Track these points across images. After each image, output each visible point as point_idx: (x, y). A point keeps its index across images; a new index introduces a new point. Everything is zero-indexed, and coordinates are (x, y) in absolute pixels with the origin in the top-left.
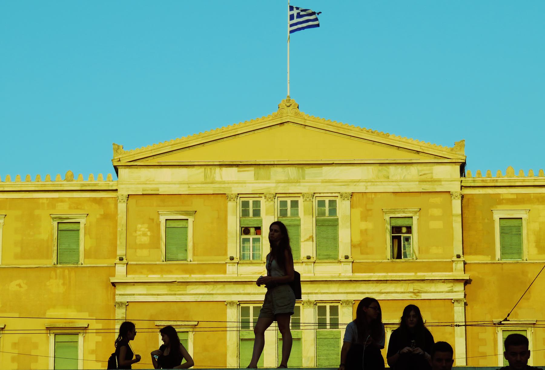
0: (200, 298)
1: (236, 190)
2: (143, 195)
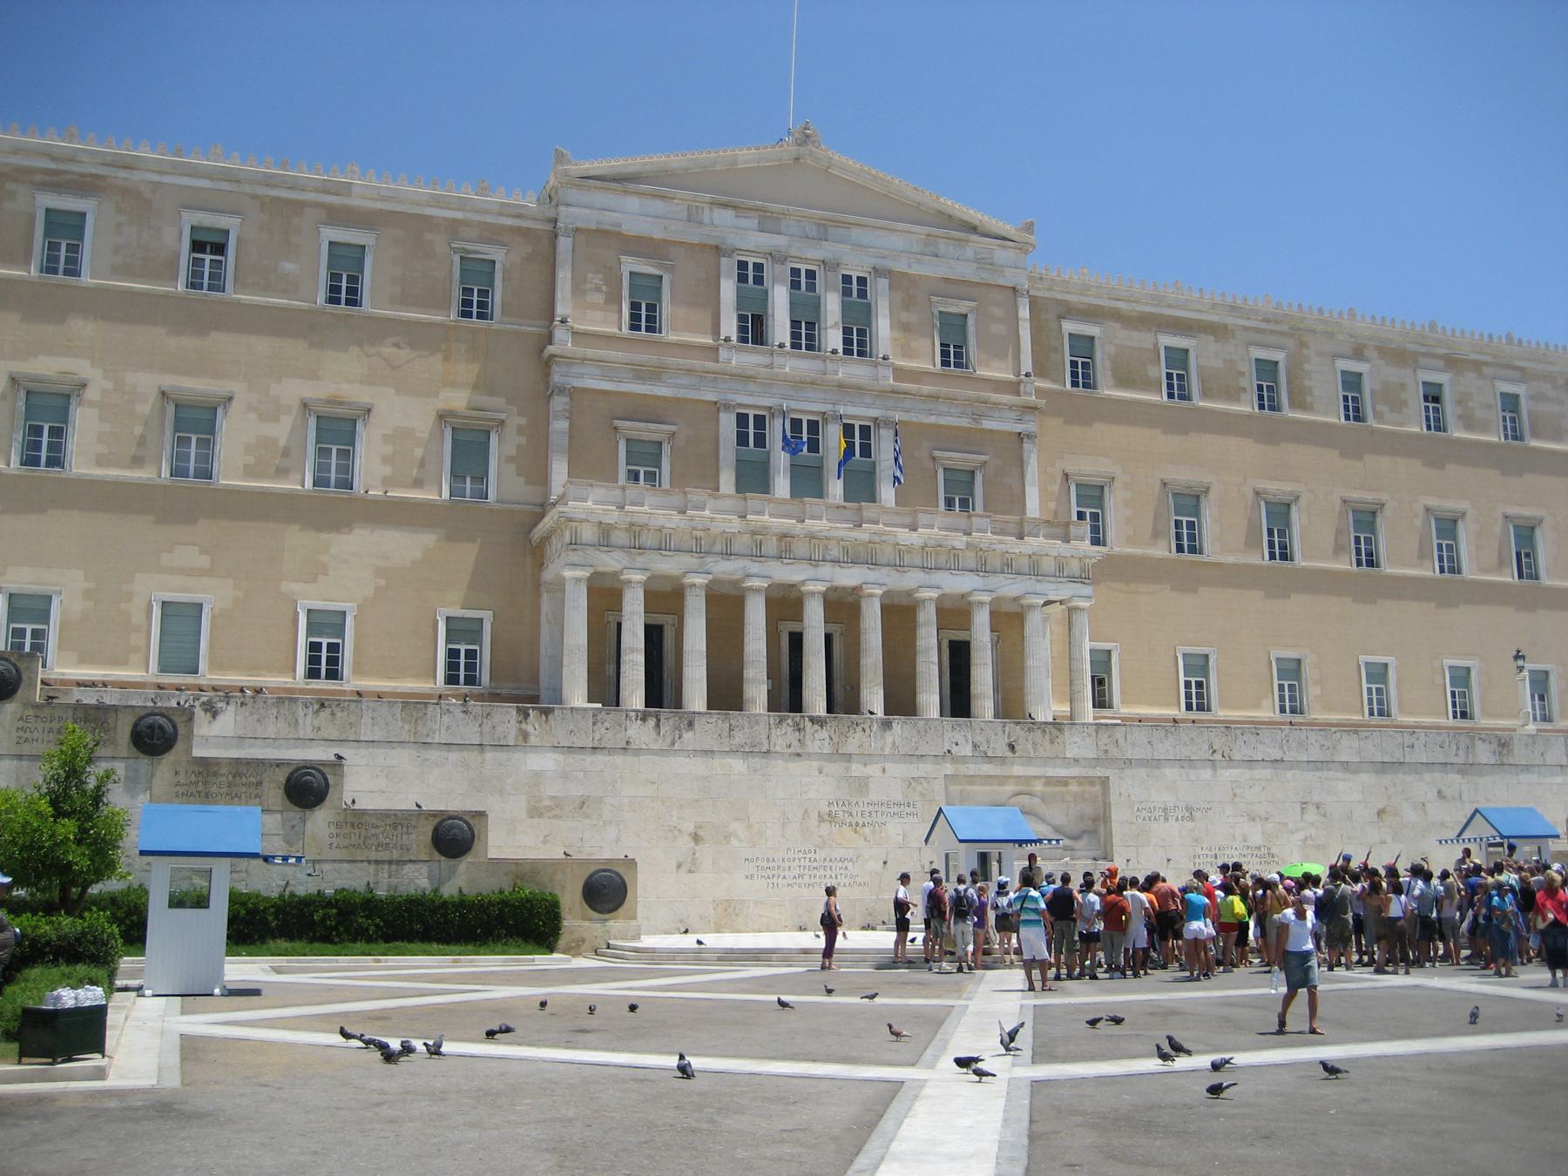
0: (681, 393)
1: (732, 240)
2: (597, 231)
